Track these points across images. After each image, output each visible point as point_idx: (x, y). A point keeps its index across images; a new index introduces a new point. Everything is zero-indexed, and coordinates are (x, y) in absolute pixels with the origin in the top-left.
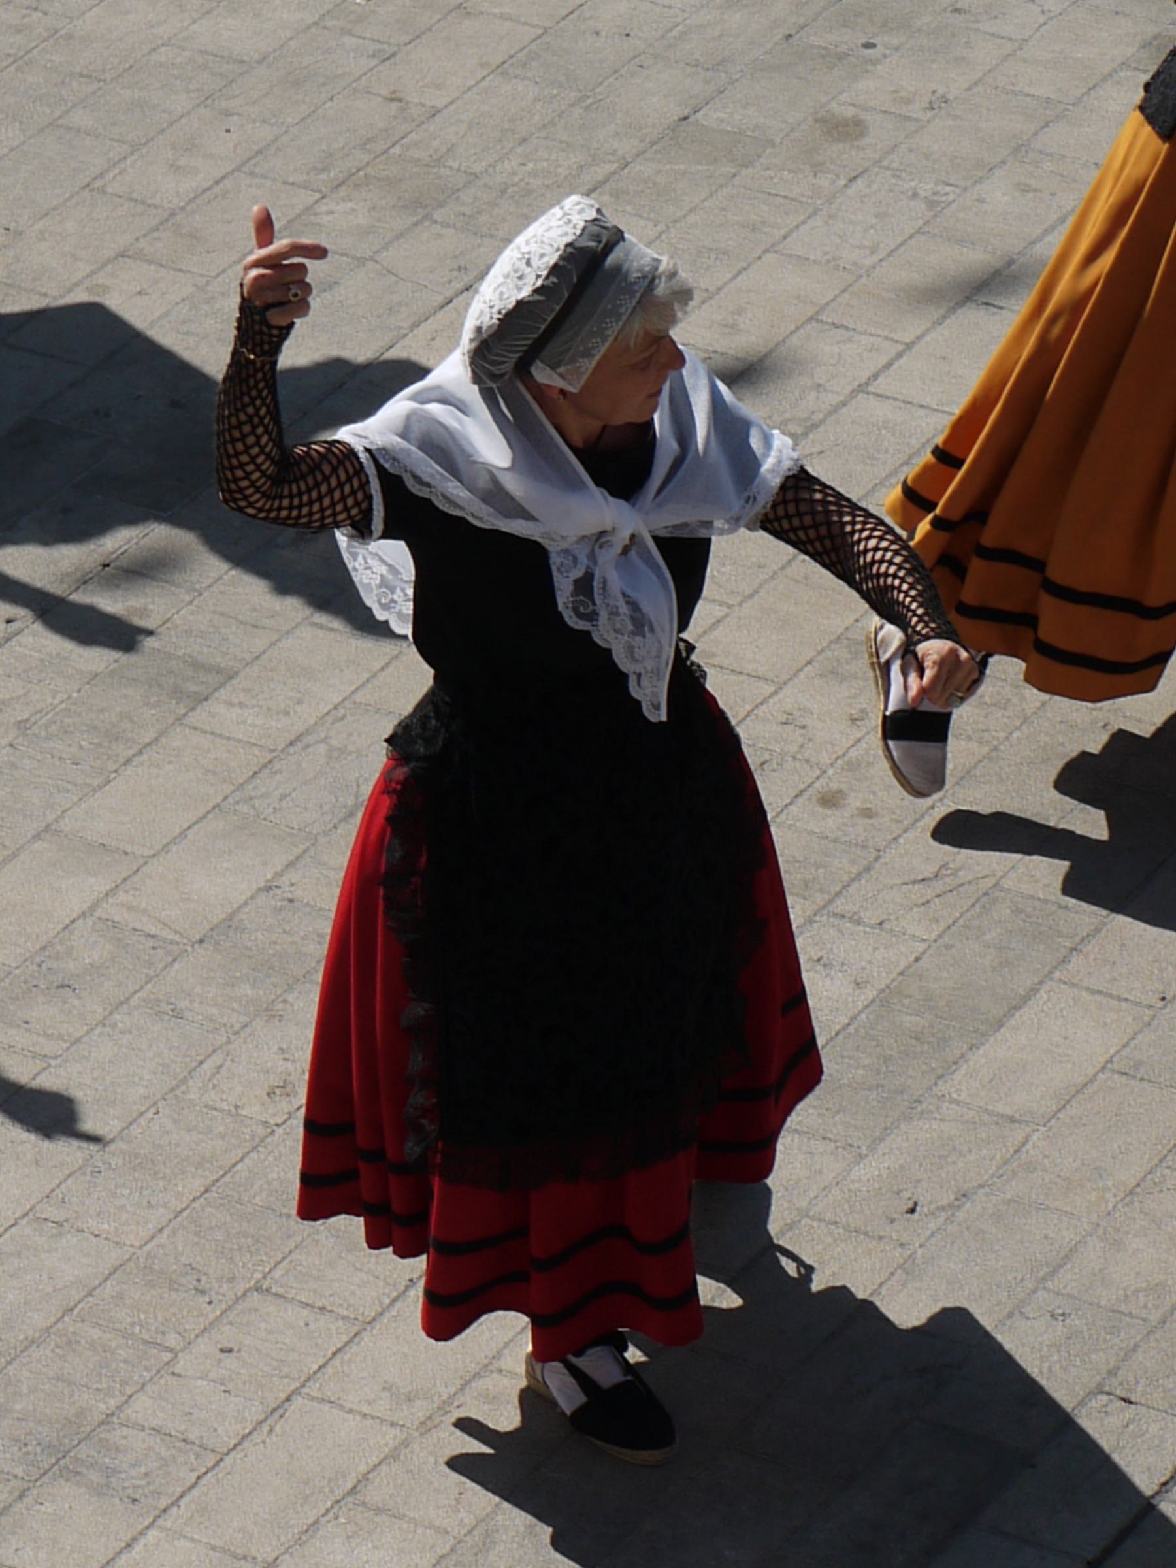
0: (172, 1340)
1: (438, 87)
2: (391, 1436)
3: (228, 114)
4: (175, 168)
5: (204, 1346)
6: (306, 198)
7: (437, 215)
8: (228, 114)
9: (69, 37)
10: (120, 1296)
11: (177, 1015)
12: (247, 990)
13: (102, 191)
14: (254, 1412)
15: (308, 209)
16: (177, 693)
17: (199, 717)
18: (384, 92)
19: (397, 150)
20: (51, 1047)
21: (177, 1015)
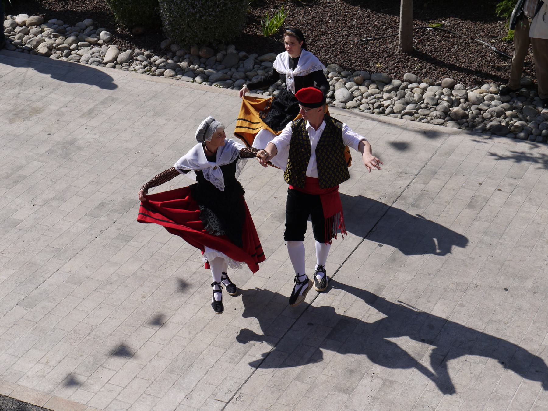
0: (130, 334)
1: (159, 151)
2: (162, 346)
3: (128, 157)
4: (121, 165)
5: (134, 334)
6: (140, 169)
7: (159, 170)
8: (128, 157)
9: (105, 147)
10: (122, 328)
11: (128, 287)
12: (138, 283)
13: (111, 169)
14: (142, 344)
15: (141, 170)
16: (126, 240)
17: (129, 244)
18: (151, 153)
19: (153, 161)
20: (110, 292)
21: (128, 287)
